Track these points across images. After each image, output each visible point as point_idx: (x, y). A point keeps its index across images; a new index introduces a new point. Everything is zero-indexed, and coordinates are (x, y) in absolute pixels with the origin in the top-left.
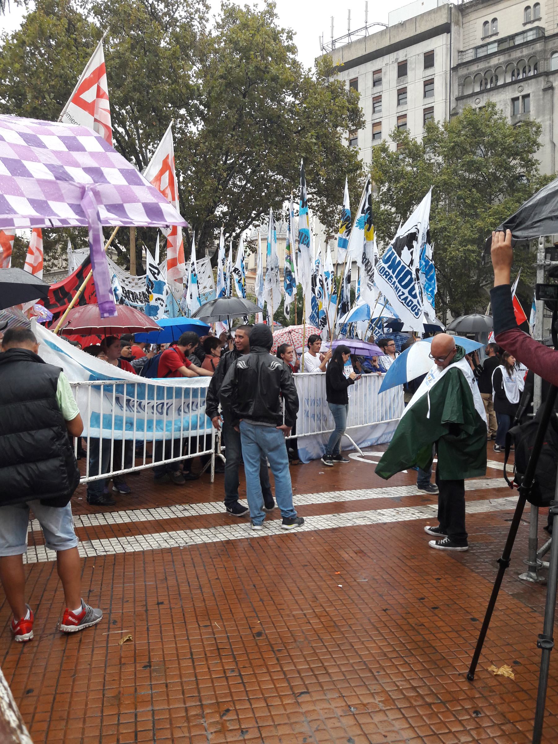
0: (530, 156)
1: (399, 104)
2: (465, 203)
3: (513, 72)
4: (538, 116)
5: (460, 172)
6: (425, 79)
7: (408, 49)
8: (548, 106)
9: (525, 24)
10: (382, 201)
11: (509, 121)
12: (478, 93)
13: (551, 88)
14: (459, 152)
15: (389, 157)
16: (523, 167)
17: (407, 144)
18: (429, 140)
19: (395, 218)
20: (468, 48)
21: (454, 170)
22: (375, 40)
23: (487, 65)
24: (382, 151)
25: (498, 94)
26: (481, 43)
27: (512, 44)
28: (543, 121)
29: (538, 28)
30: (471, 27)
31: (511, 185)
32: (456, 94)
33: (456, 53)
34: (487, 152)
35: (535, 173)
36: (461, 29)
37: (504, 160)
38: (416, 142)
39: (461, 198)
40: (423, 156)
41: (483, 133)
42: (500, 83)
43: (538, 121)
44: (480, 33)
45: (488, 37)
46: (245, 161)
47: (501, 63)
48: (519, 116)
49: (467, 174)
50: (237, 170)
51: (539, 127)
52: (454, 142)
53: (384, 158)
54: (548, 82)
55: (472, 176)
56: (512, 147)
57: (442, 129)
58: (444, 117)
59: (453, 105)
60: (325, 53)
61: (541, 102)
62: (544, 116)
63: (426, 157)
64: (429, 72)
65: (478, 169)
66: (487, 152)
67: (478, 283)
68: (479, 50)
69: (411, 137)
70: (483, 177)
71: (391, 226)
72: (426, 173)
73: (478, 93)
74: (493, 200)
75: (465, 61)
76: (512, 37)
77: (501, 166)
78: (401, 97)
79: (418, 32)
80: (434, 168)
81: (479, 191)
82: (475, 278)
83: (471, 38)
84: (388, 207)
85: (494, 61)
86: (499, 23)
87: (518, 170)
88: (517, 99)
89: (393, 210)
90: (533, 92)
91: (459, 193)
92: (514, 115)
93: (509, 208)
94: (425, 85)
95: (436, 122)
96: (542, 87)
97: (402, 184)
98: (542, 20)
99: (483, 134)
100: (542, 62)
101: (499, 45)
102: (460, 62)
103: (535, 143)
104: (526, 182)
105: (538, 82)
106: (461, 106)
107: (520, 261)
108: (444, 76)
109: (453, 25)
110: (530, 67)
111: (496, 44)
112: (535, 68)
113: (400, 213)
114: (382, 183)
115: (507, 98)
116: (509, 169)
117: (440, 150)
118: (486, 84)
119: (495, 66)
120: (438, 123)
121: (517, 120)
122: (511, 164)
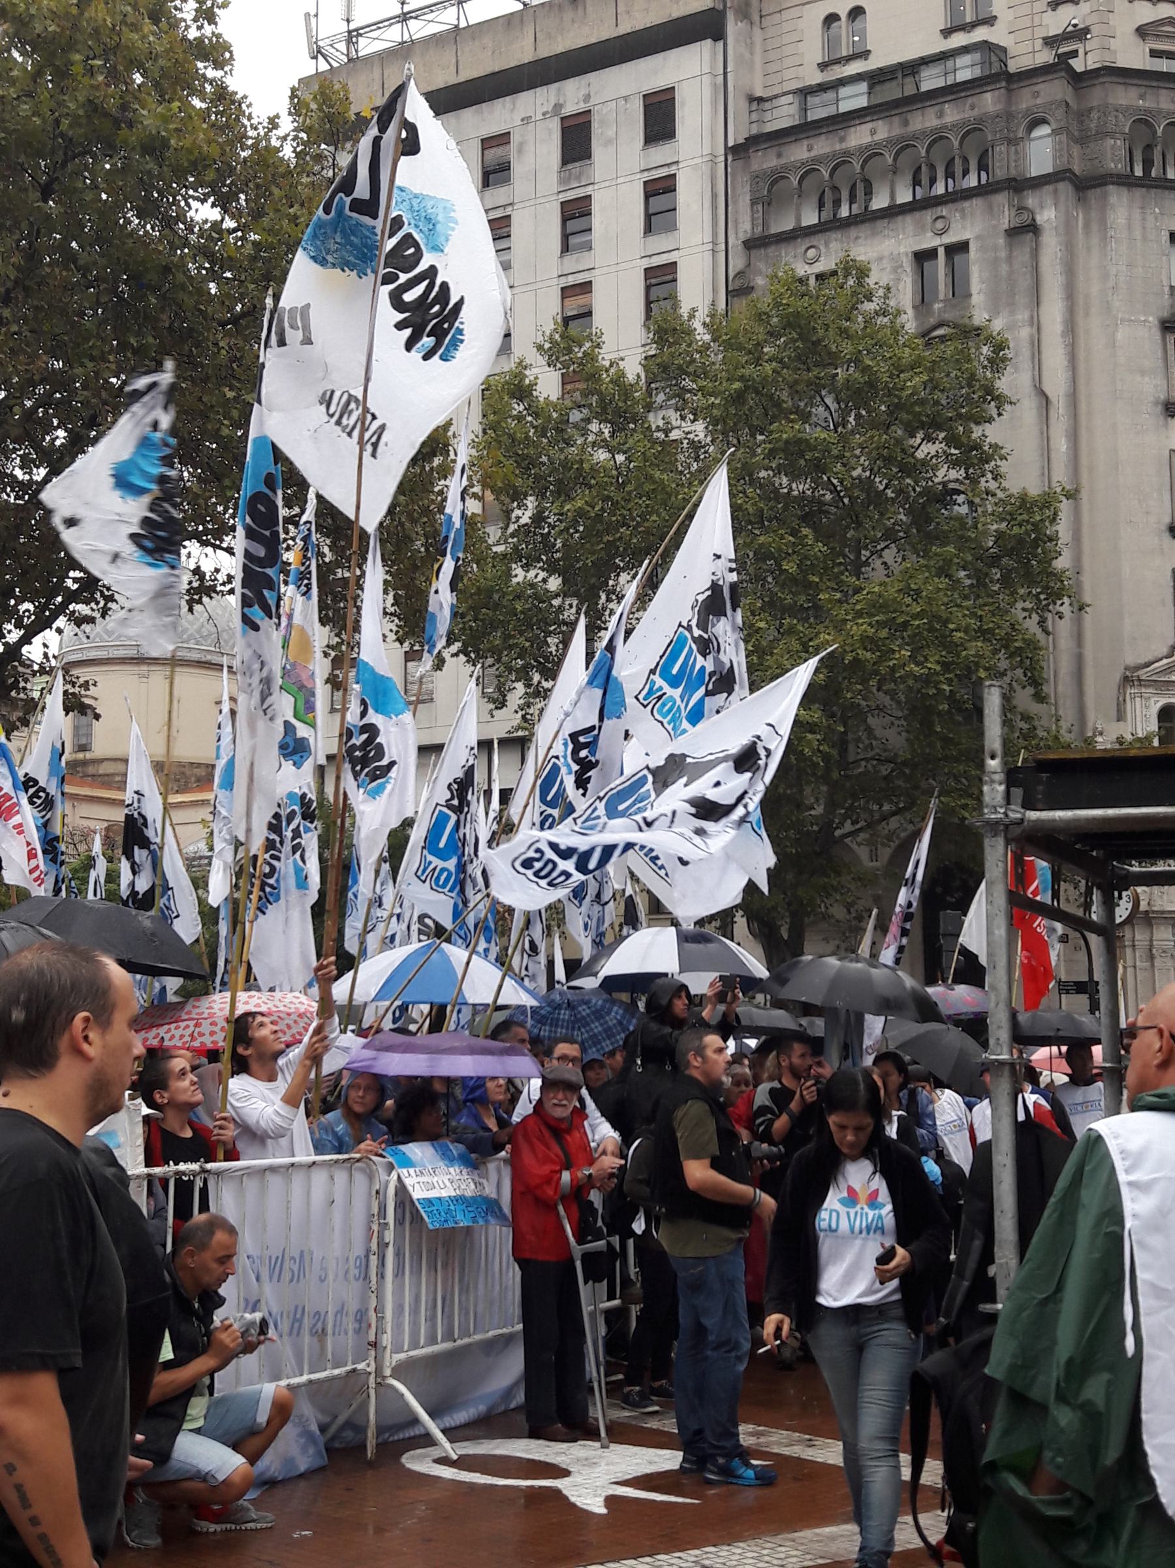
0: (977, 432)
1: (566, 248)
2: (782, 571)
3: (918, 171)
4: (995, 311)
5: (763, 474)
6: (647, 176)
7: (592, 77)
8: (1025, 282)
9: (947, 33)
10: (516, 555)
11: (909, 323)
12: (811, 231)
13: (1032, 228)
14: (759, 412)
15: (536, 415)
16: (955, 464)
17: (594, 377)
18: (664, 368)
19: (561, 609)
20: (777, 90)
21: (745, 465)
22: (487, 41)
23: (838, 147)
24: (513, 396)
25: (874, 234)
26: (817, 78)
27: (910, 90)
28: (1011, 327)
29: (986, 47)
30: (786, 27)
31: (920, 517)
32: (745, 227)
33: (744, 104)
34: (845, 413)
35: (993, 485)
36: (756, 30)
37: (898, 442)
38: (622, 374)
39: (769, 556)
40: (645, 420)
41: (830, 353)
42: (880, 202)
43: (997, 325)
44: (812, 49)
45: (837, 62)
46: (45, 402)
47: (877, 144)
48: (936, 306)
49: (785, 480)
50: (15, 432)
51: (1000, 347)
52: (742, 378)
53: (520, 418)
54: (1021, 208)
55: (800, 487)
56: (922, 402)
57: (702, 335)
58: (709, 298)
59: (737, 264)
60: (323, 66)
61: (1004, 268)
62: (1012, 313)
63: (655, 420)
64: (661, 154)
65: (818, 468)
66: (845, 413)
67: (827, 827)
68: (813, 100)
69: (606, 355)
70: (834, 490)
71: (549, 634)
72: (657, 474)
73: (811, 231)
74: (867, 563)
75: (769, 128)
76: (912, 68)
77: (888, 460)
78: (572, 225)
79: (625, 28)
80: (681, 457)
81: (820, 536)
82: (819, 810)
83: (788, 62)
84: (536, 574)
85: (860, 136)
86: (872, 23)
87: (941, 473)
88: (931, 254)
89: (554, 583)
90: (978, 238)
91: (762, 539)
92: (923, 301)
93: (918, 592)
94: (648, 196)
95: (684, 311)
96: (1006, 226)
97: (579, 503)
98: (999, 25)
99: (833, 360)
100: (1001, 149)
101: (871, 87)
102: (755, 130)
103: (989, 391)
104: (964, 510)
105: (991, 208)
106: (761, 266)
107: (957, 760)
108: (706, 169)
109: (730, 17)
110: (965, 160)
111: (863, 87)
112: (983, 166)
113: (576, 594)
114: (518, 496)
115: (902, 250)
116: (914, 468)
117: (697, 400)
118: (837, 203)
119: (862, 149)
120: (692, 316)
121: (932, 321)
122: (920, 455)
